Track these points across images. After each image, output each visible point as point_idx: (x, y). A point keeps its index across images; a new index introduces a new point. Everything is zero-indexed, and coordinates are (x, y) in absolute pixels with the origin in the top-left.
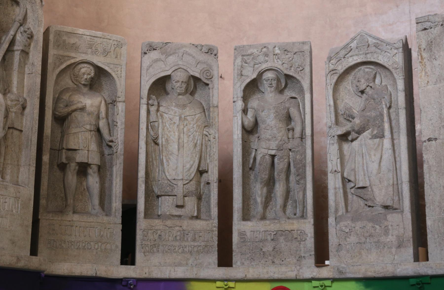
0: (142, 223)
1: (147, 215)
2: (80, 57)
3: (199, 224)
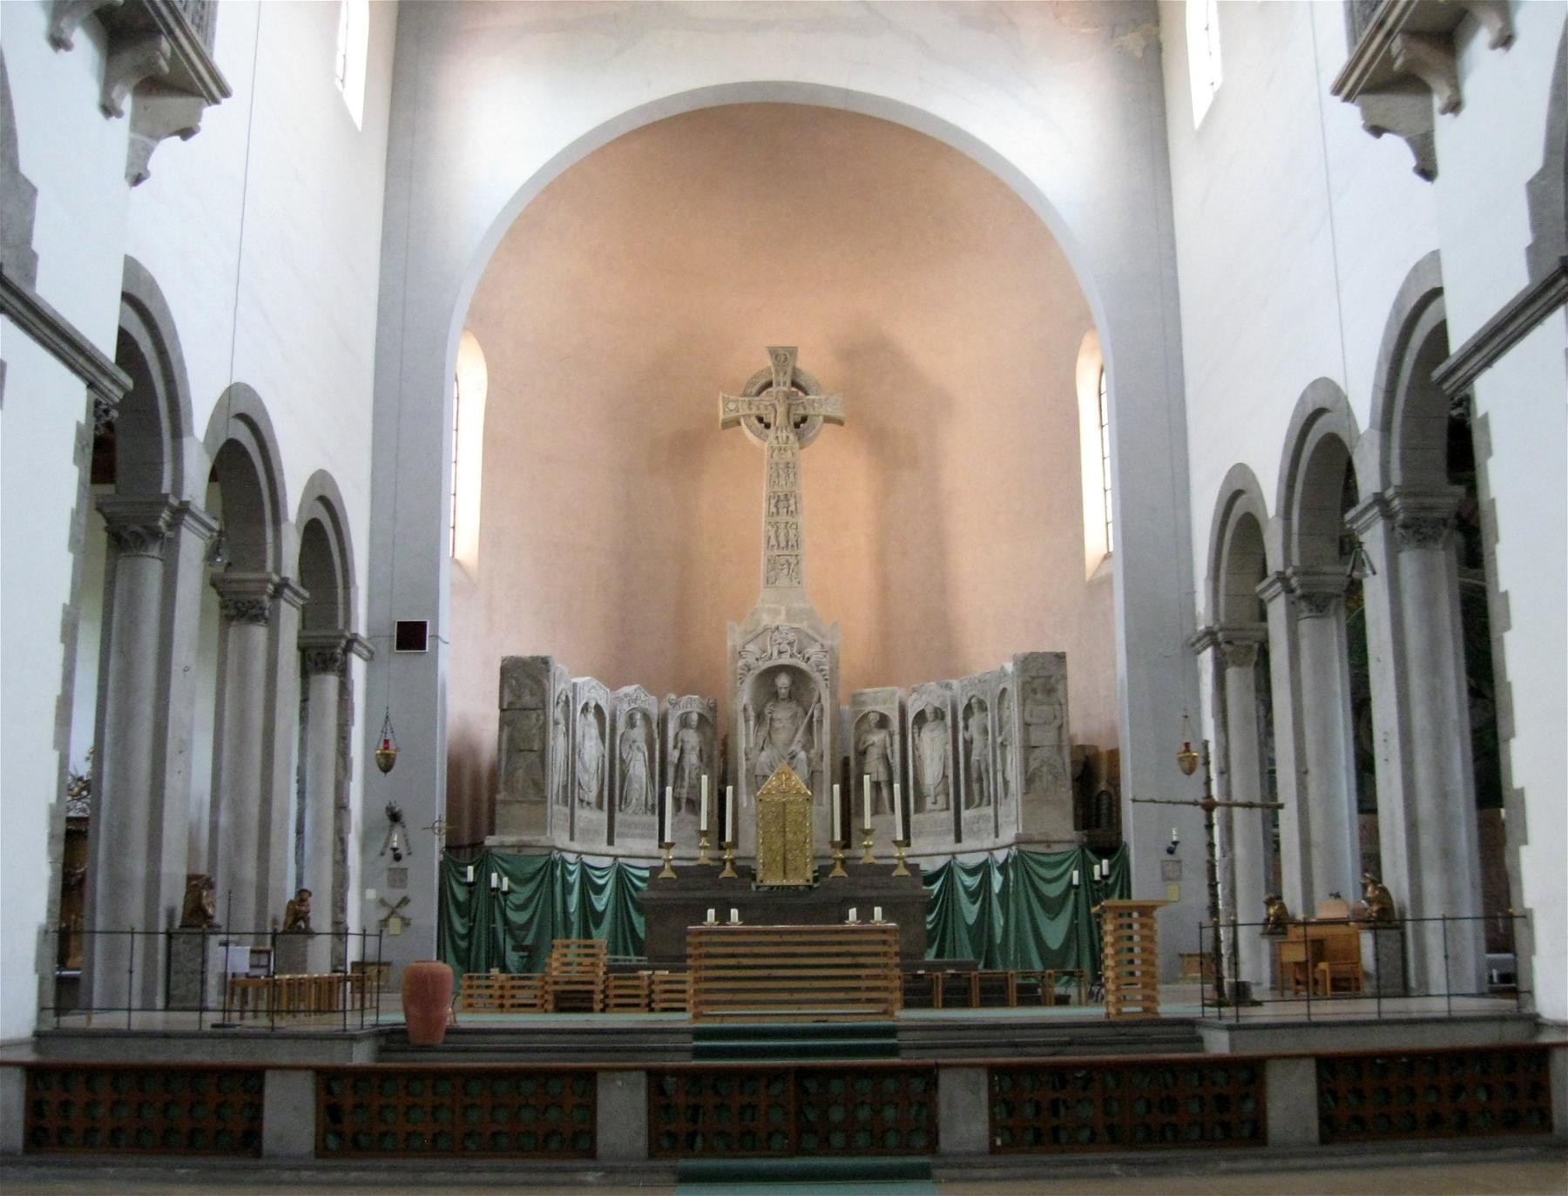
0: (913, 818)
1: (916, 811)
2: (867, 709)
3: (944, 815)
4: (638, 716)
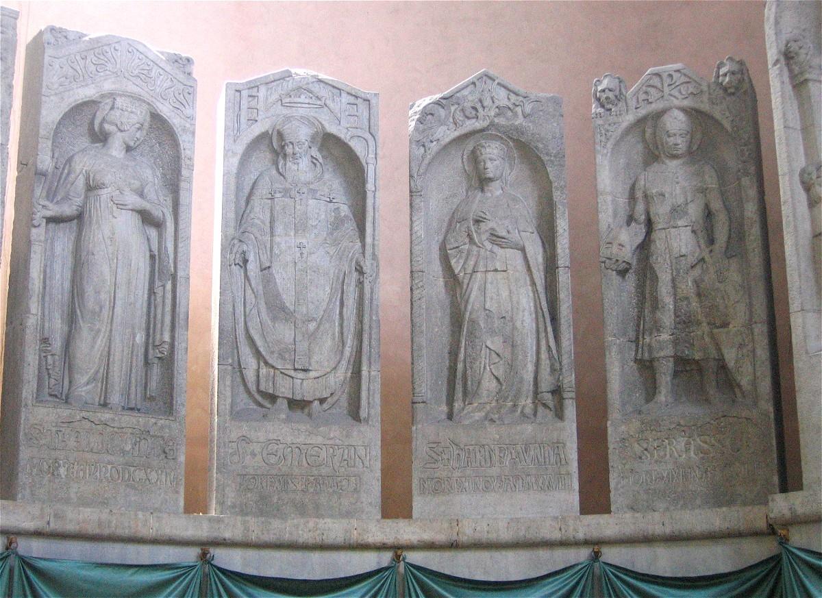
4: (493, 152)
